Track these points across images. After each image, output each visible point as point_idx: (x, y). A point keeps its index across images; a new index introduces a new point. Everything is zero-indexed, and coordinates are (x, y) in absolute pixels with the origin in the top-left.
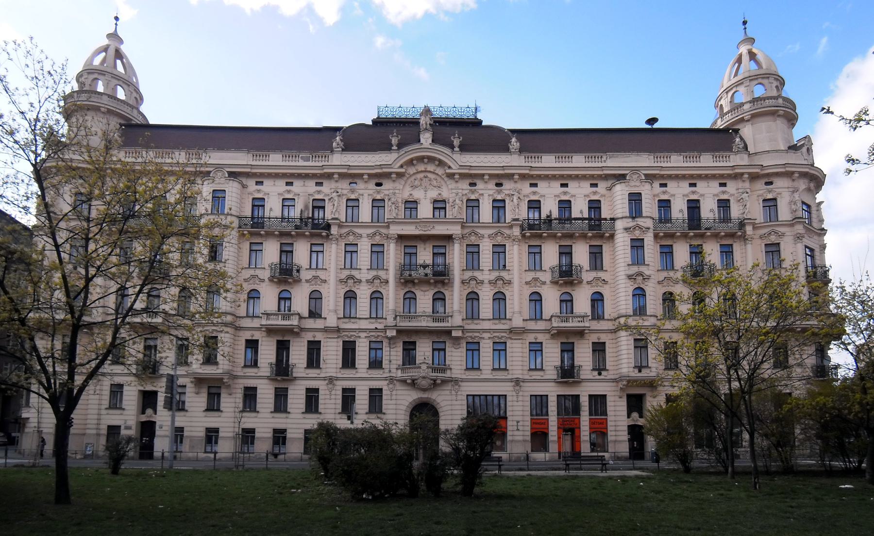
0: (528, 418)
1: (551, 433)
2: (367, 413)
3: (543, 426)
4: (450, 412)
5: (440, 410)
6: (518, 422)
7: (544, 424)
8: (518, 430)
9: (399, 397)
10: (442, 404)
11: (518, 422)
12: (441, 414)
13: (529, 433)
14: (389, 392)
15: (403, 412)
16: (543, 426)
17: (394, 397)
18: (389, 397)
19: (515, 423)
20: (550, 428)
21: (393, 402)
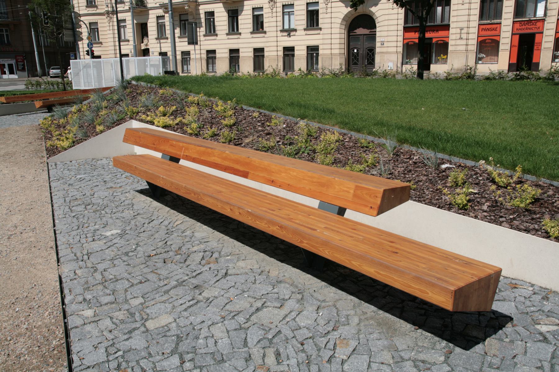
1: (502, 41)
2: (305, 30)
3: (493, 33)
4: (386, 23)
5: (376, 21)
6: (462, 29)
7: (495, 29)
8: (461, 38)
9: (333, 10)
10: (377, 14)
11: (462, 29)
12: (377, 25)
13: (475, 42)
14: (324, 5)
15: (339, 26)
16: (493, 33)
17: (329, 10)
18: (325, 11)
19: (459, 31)
20: (503, 35)
21: (329, 15)
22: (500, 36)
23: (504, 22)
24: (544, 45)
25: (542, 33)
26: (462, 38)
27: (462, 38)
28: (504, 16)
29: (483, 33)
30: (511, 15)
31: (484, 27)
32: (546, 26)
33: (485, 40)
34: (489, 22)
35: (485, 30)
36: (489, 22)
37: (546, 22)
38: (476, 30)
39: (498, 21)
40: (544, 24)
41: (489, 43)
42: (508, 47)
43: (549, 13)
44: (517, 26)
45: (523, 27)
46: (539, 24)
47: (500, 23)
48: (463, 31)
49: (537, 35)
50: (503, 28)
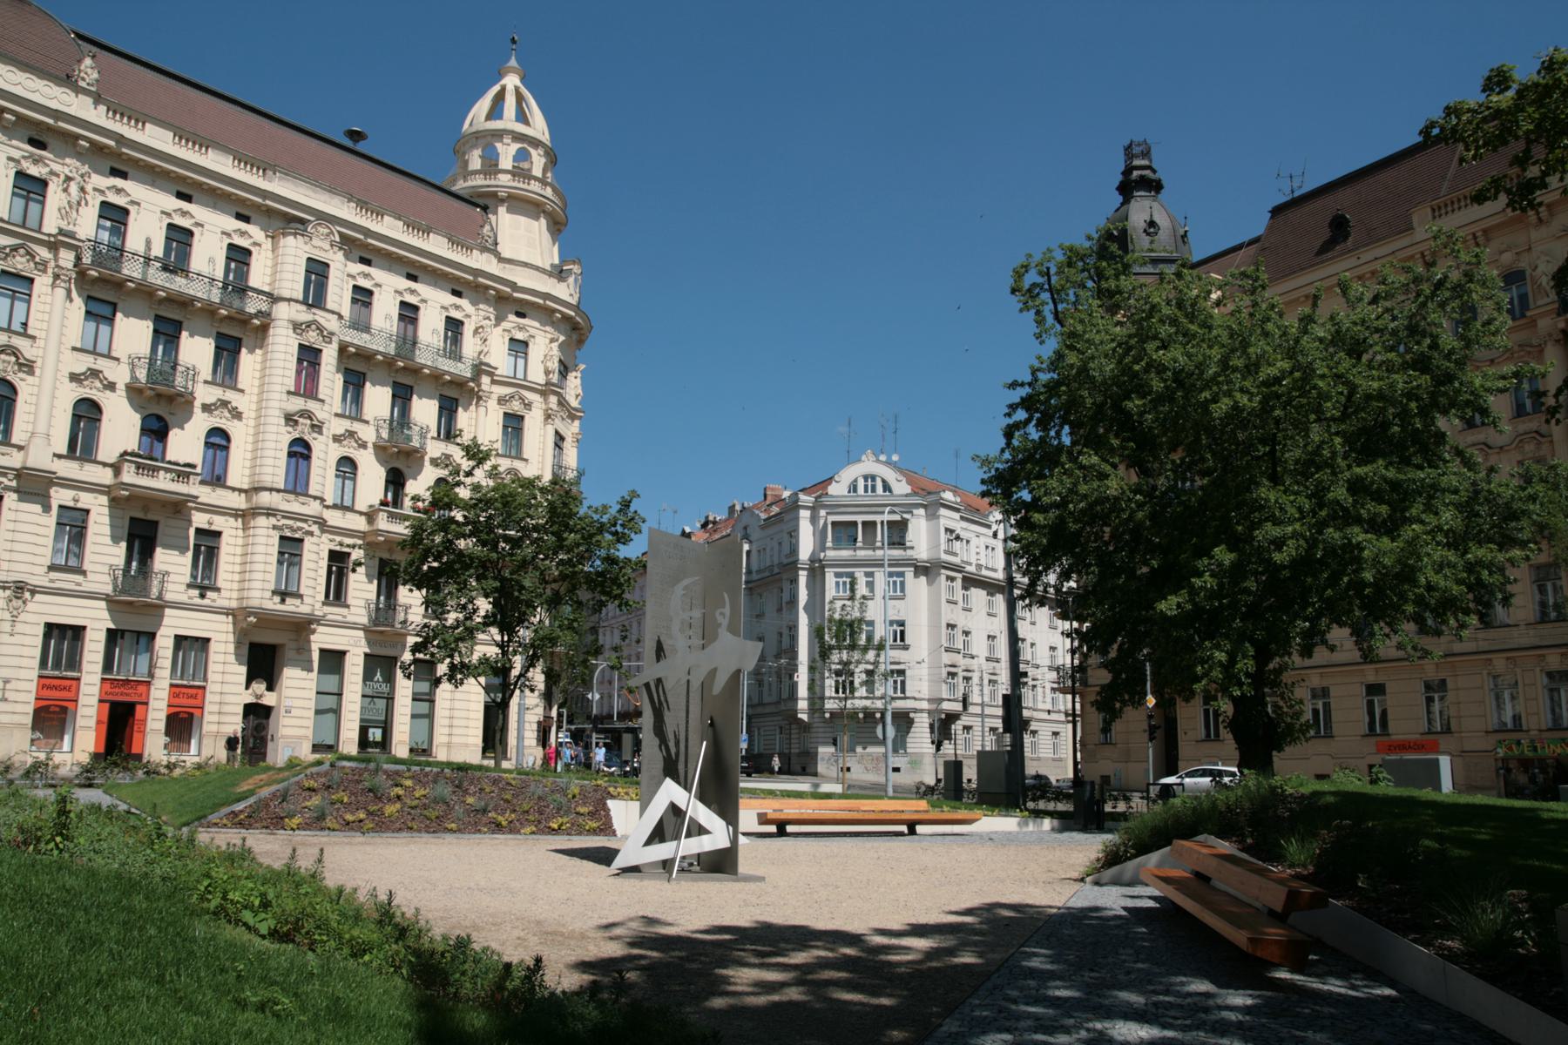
0: (34, 674)
7: (194, 697)
13: (30, 709)
16: (192, 702)
20: (82, 700)
22: (76, 701)
23: (85, 679)
24: (151, 725)
25: (146, 704)
26: (6, 700)
27: (6, 700)
28: (86, 666)
29: (176, 701)
30: (99, 667)
31: (177, 690)
32: (154, 693)
33: (49, 706)
34: (56, 673)
35: (49, 687)
36: (56, 673)
37: (152, 688)
38: (33, 686)
39: (75, 674)
40: (149, 690)
41: (54, 712)
42: (92, 723)
43: (158, 672)
44: (107, 686)
45: (117, 690)
46: (141, 689)
47: (78, 679)
48: (8, 686)
49: (138, 707)
50: (84, 689)
